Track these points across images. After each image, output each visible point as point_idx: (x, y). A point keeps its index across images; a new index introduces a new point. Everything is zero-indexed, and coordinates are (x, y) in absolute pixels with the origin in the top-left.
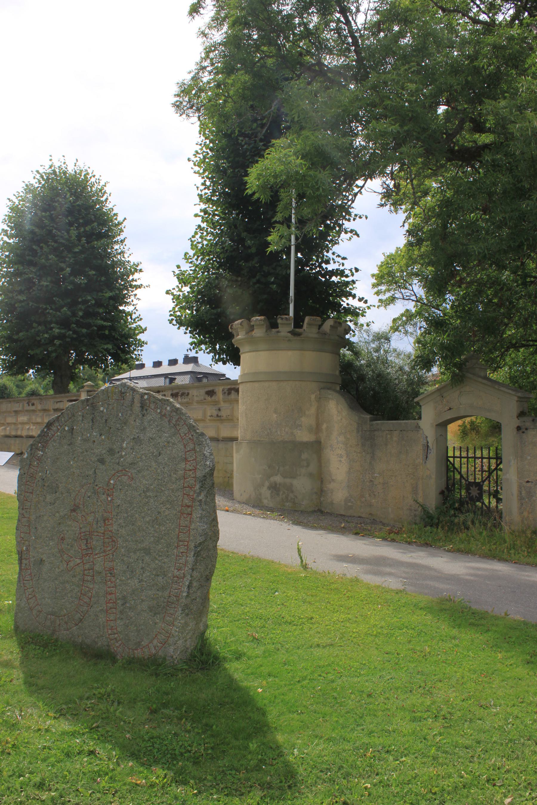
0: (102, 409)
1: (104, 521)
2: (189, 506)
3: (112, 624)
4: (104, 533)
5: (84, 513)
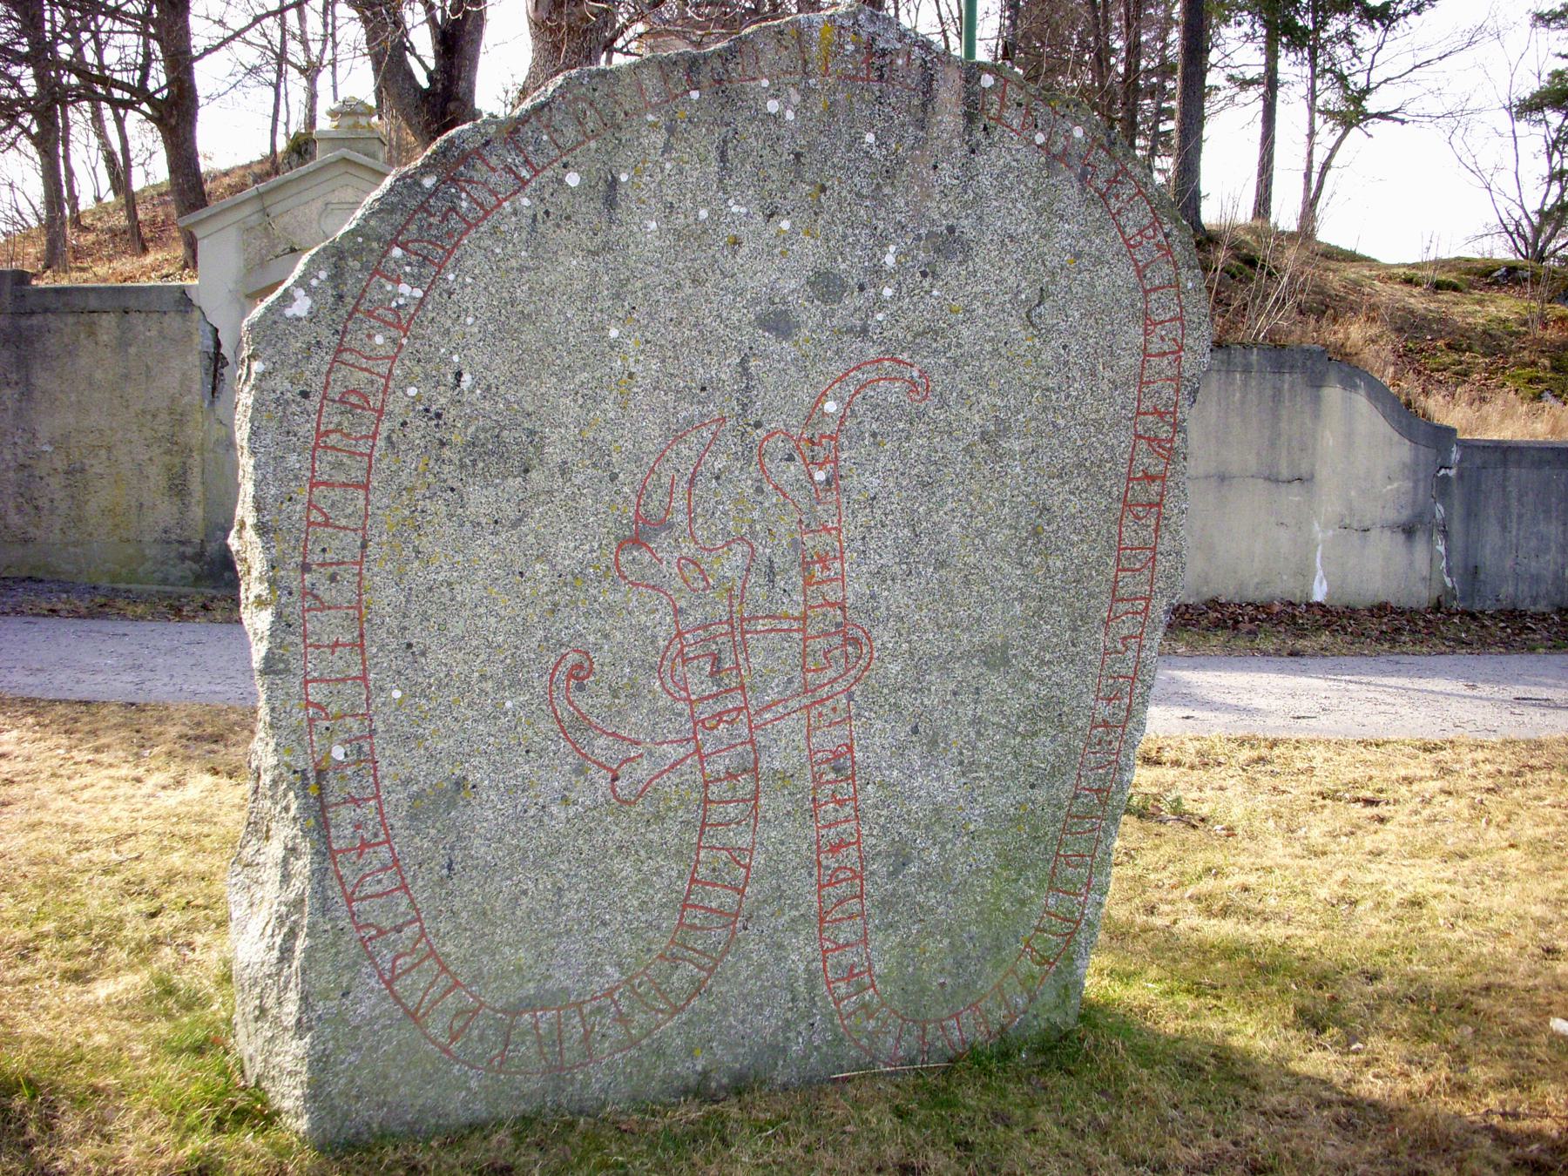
0: (773, 106)
1: (806, 566)
2: (1152, 479)
3: (850, 957)
4: (804, 617)
5: (688, 549)
